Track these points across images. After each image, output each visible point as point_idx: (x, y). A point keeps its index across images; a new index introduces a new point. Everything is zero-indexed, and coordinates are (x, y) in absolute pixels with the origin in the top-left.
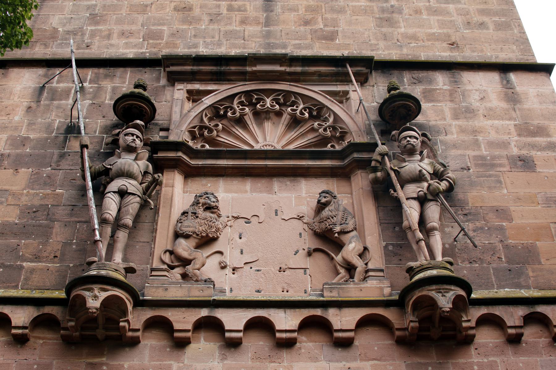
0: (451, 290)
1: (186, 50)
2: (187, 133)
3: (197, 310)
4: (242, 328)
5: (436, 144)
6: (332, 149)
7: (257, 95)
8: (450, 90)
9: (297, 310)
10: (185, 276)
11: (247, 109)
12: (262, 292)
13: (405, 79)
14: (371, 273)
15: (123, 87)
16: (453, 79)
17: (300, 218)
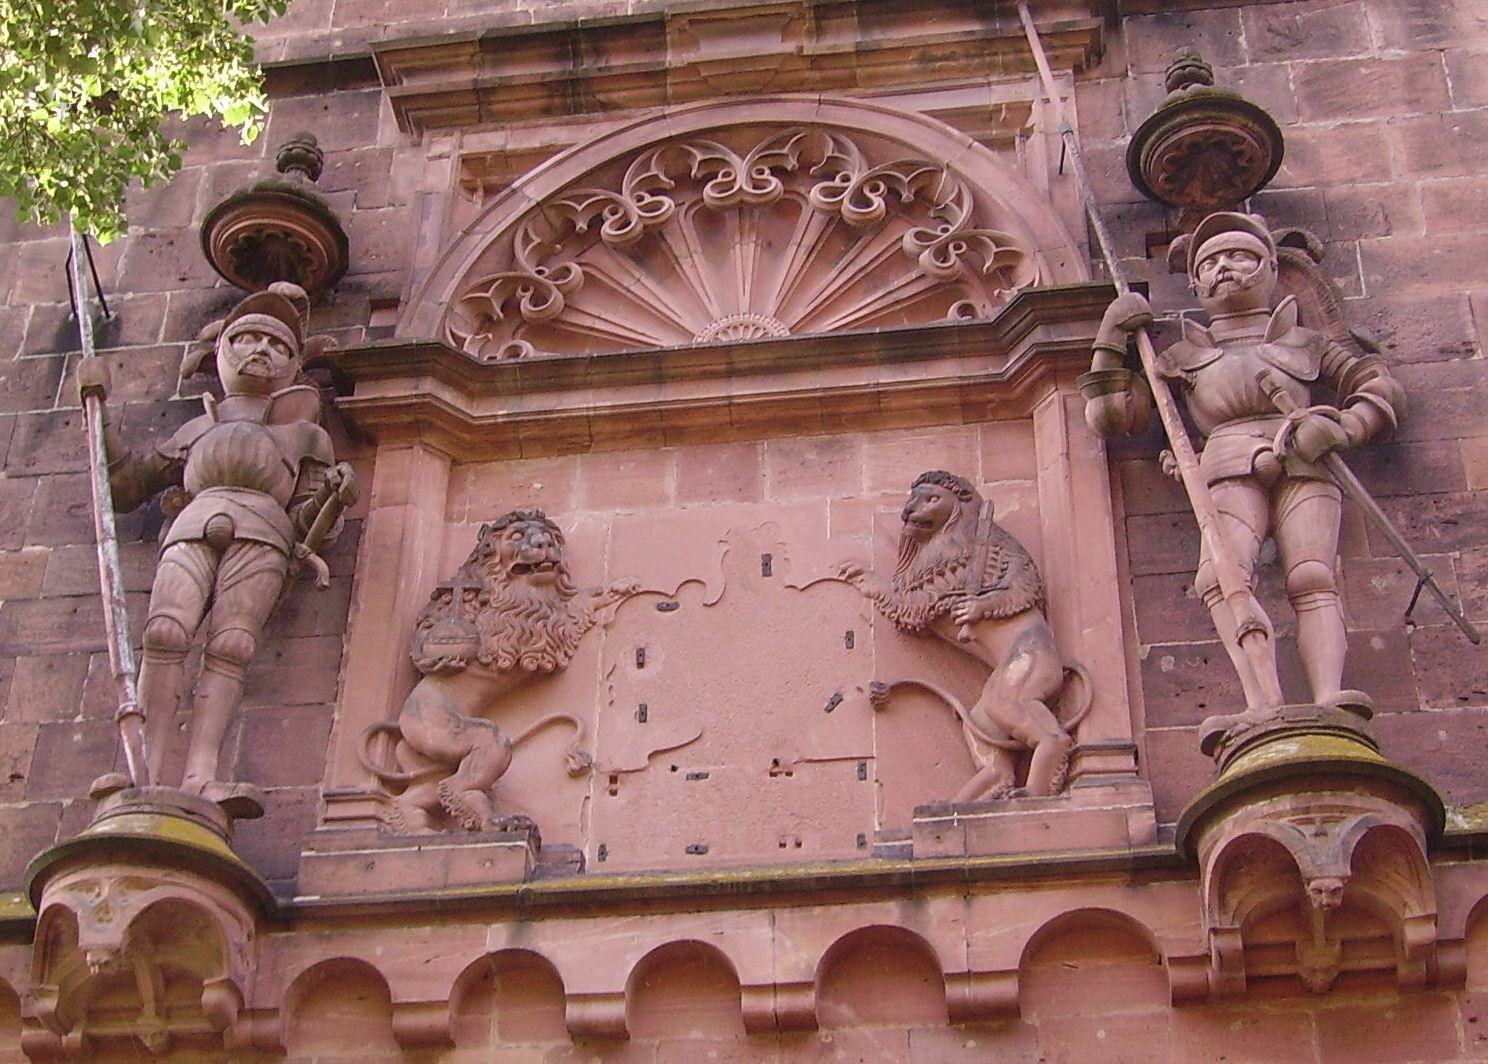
0: (1350, 809)
1: (470, 14)
2: (459, 309)
3: (472, 928)
4: (620, 984)
5: (1347, 268)
6: (966, 320)
7: (706, 148)
8: (1407, 64)
9: (818, 910)
10: (438, 814)
11: (667, 202)
12: (711, 852)
13: (1242, 39)
15: (250, 168)
16: (1420, 22)
17: (850, 578)
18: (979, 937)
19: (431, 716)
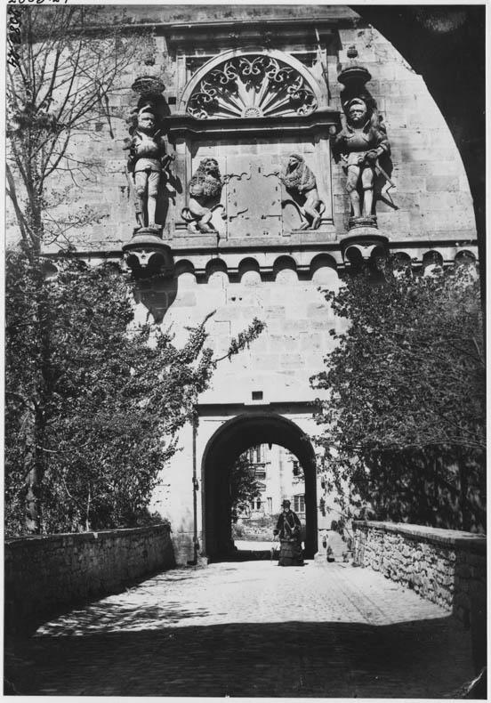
14: (323, 222)
17: (277, 174)
18: (304, 259)
19: (195, 207)
